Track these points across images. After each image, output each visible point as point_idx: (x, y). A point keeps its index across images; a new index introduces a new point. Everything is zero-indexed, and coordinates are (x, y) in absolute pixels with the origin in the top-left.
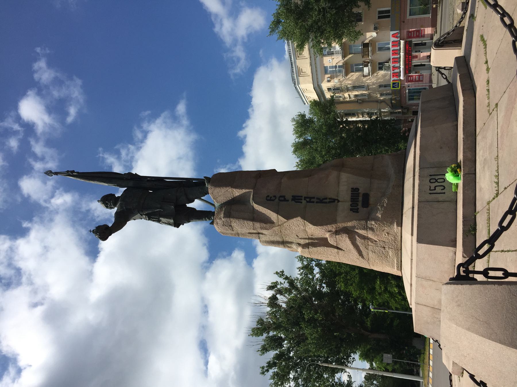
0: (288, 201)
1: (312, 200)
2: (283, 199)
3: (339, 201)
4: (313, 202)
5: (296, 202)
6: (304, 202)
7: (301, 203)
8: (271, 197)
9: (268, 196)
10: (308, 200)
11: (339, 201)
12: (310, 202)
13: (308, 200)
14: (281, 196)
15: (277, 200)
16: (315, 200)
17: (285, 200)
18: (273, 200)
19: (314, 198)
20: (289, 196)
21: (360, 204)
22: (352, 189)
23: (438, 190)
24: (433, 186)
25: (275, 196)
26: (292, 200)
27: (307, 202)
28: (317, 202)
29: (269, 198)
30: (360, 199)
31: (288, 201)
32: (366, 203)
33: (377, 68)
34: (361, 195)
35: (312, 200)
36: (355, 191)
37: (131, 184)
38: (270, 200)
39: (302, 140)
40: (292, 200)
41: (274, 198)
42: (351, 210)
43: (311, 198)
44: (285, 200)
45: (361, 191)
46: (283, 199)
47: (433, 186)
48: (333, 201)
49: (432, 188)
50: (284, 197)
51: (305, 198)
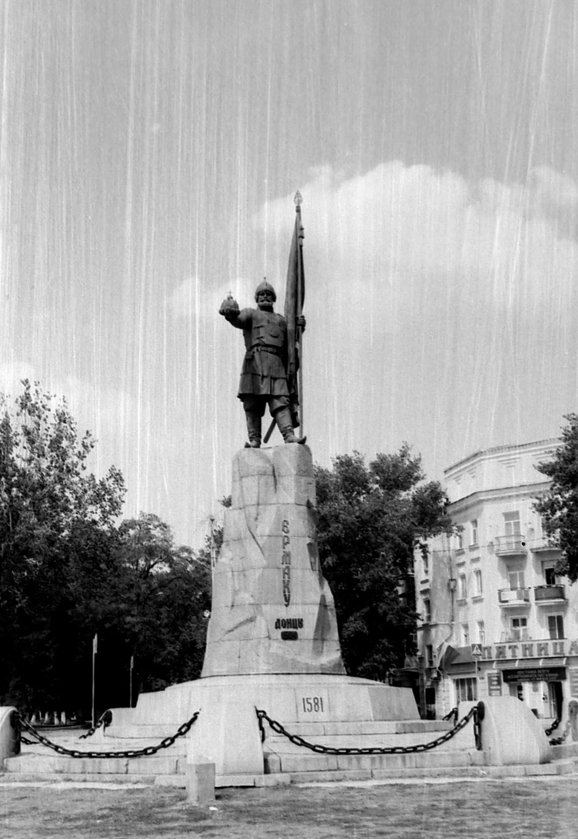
3: (287, 606)
6: (284, 566)
11: (287, 606)
20: (288, 548)
21: (286, 630)
23: (308, 706)
24: (311, 701)
28: (284, 582)
32: (287, 636)
33: (515, 617)
36: (299, 623)
37: (290, 327)
39: (367, 468)
42: (278, 620)
45: (299, 631)
47: (311, 701)
48: (287, 600)
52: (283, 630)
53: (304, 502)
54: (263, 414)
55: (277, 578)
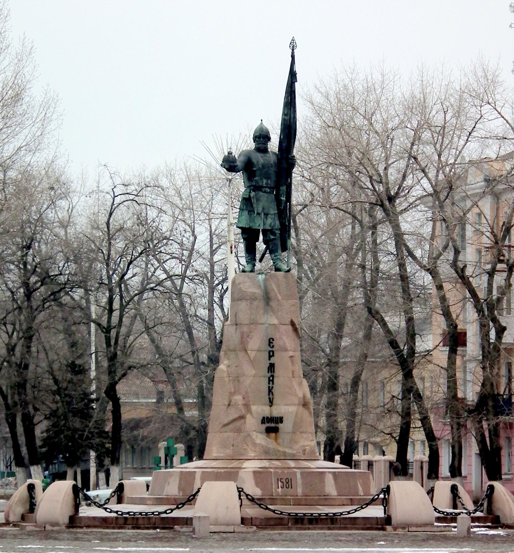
0: (270, 359)
1: (271, 383)
2: (271, 354)
3: (271, 406)
4: (269, 384)
5: (268, 368)
7: (268, 372)
8: (272, 343)
9: (273, 340)
10: (271, 378)
11: (271, 406)
12: (269, 380)
13: (271, 378)
14: (273, 352)
15: (271, 349)
16: (271, 385)
17: (270, 357)
18: (269, 345)
19: (273, 384)
20: (273, 360)
22: (282, 417)
24: (284, 481)
25: (273, 346)
26: (270, 364)
27: (269, 378)
28: (269, 387)
29: (271, 340)
30: (273, 425)
31: (270, 359)
34: (277, 425)
35: (271, 383)
36: (280, 420)
38: (270, 343)
40: (270, 364)
41: (271, 345)
42: (264, 418)
43: (273, 381)
44: (270, 357)
45: (280, 426)
46: (271, 354)
47: (284, 481)
49: (282, 480)
50: (273, 355)
51: (273, 376)
52: (268, 425)
53: (288, 321)
54: (258, 241)
55: (264, 385)
